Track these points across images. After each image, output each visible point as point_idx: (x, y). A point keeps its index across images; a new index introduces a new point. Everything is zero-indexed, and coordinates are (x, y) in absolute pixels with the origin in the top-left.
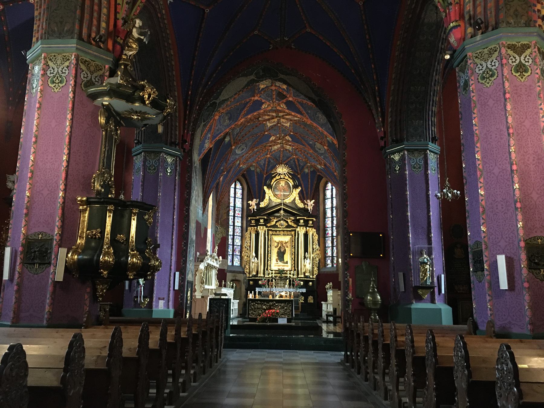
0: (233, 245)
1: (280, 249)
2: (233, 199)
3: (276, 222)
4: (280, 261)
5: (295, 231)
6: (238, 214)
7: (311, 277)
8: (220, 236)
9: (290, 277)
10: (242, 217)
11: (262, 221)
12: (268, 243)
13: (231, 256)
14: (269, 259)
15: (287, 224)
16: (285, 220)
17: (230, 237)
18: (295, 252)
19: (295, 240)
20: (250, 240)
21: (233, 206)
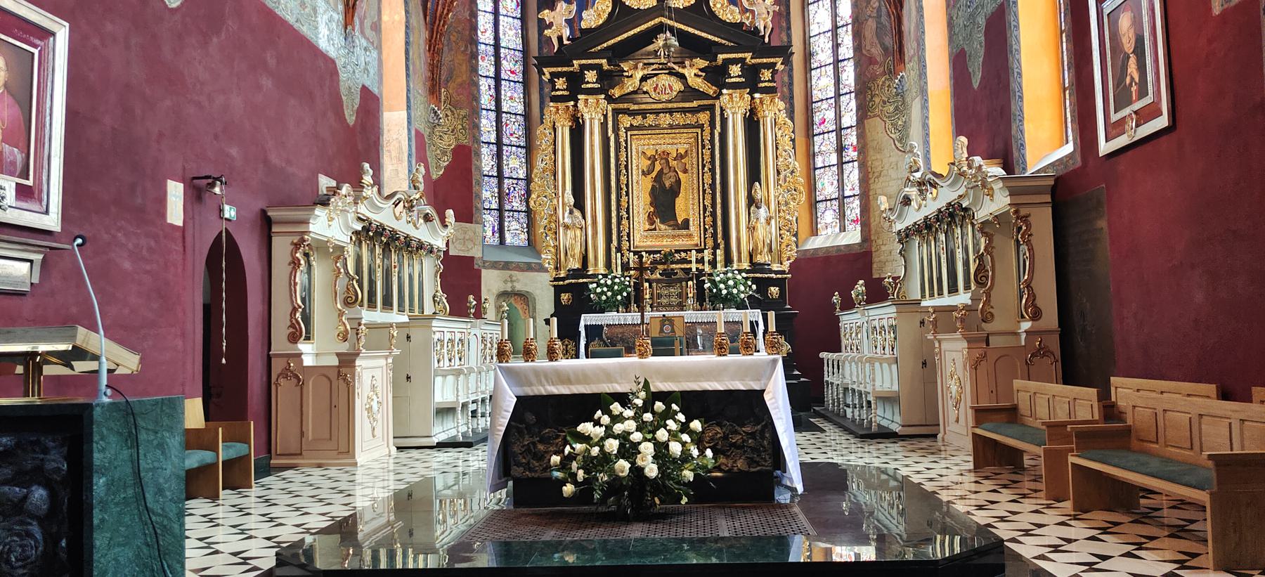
0: (500, 177)
1: (659, 178)
2: (491, 17)
3: (644, 79)
4: (662, 222)
5: (711, 108)
6: (512, 72)
7: (775, 267)
8: (449, 142)
9: (701, 272)
10: (526, 83)
11: (591, 76)
12: (617, 159)
13: (496, 213)
14: (624, 213)
15: (678, 86)
16: (672, 73)
17: (485, 150)
18: (713, 186)
19: (712, 141)
20: (555, 152)
21: (492, 42)
